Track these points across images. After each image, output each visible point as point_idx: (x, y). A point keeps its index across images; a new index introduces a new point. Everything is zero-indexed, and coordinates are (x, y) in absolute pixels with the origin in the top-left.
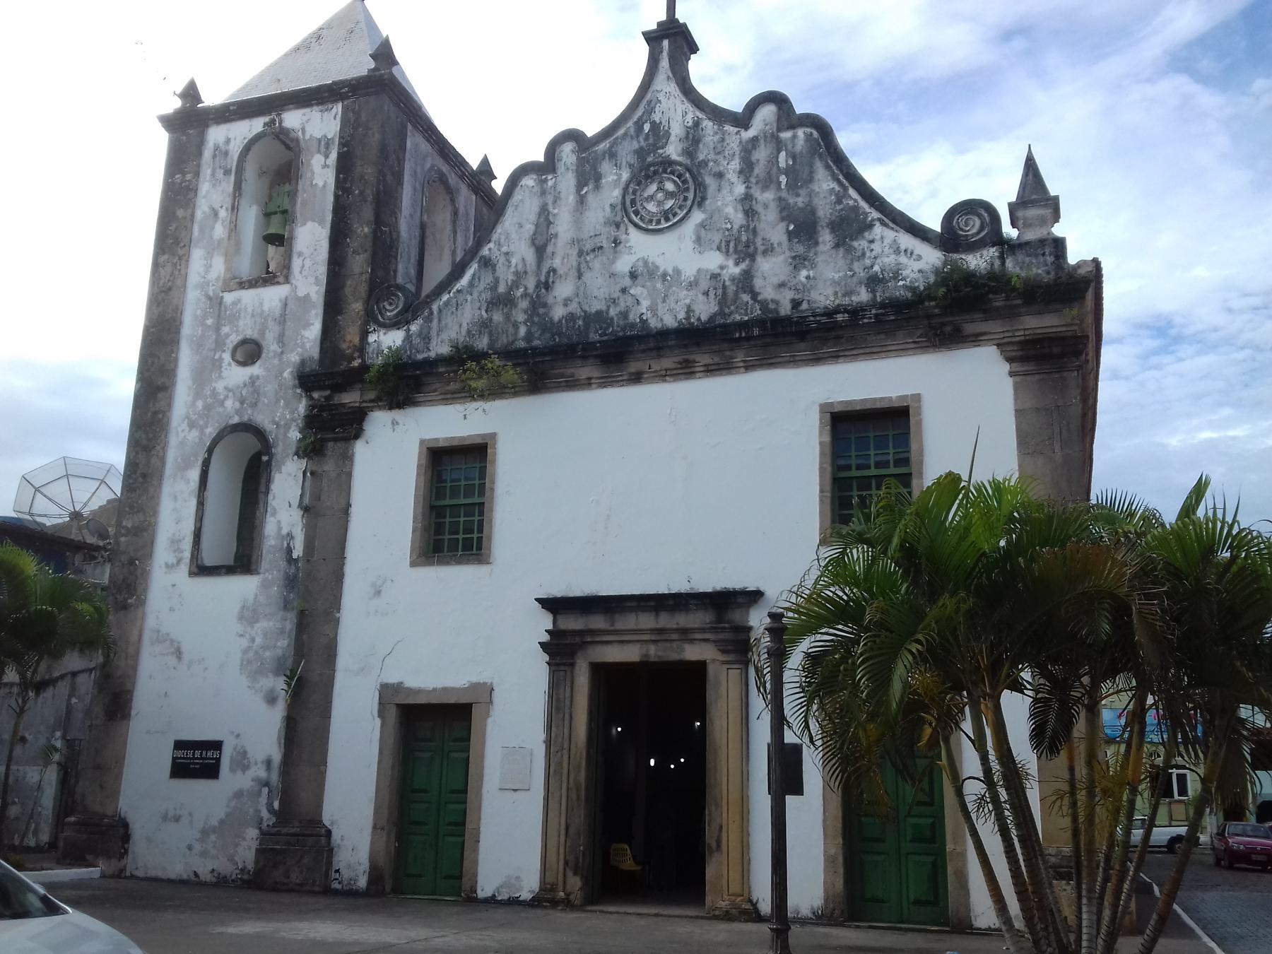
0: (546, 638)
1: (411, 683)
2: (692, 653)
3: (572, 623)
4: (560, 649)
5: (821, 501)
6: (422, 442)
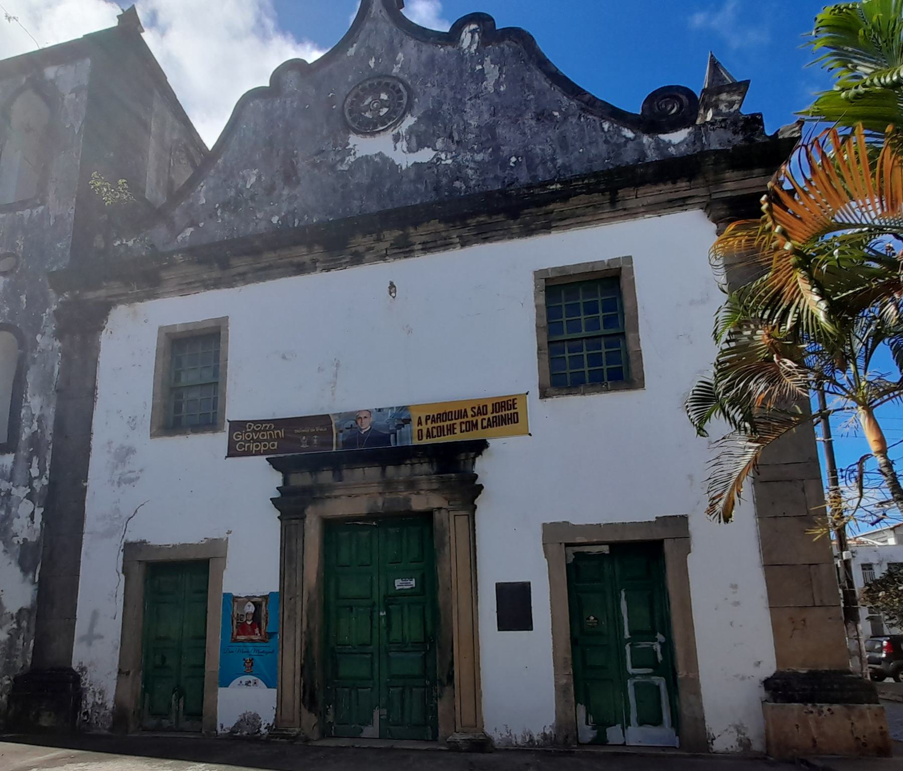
0: (277, 495)
2: (418, 503)
3: (302, 479)
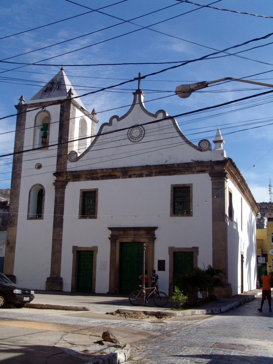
0: (110, 236)
1: (79, 246)
2: (142, 240)
3: (116, 233)
4: (113, 239)
5: (171, 207)
6: (81, 190)
